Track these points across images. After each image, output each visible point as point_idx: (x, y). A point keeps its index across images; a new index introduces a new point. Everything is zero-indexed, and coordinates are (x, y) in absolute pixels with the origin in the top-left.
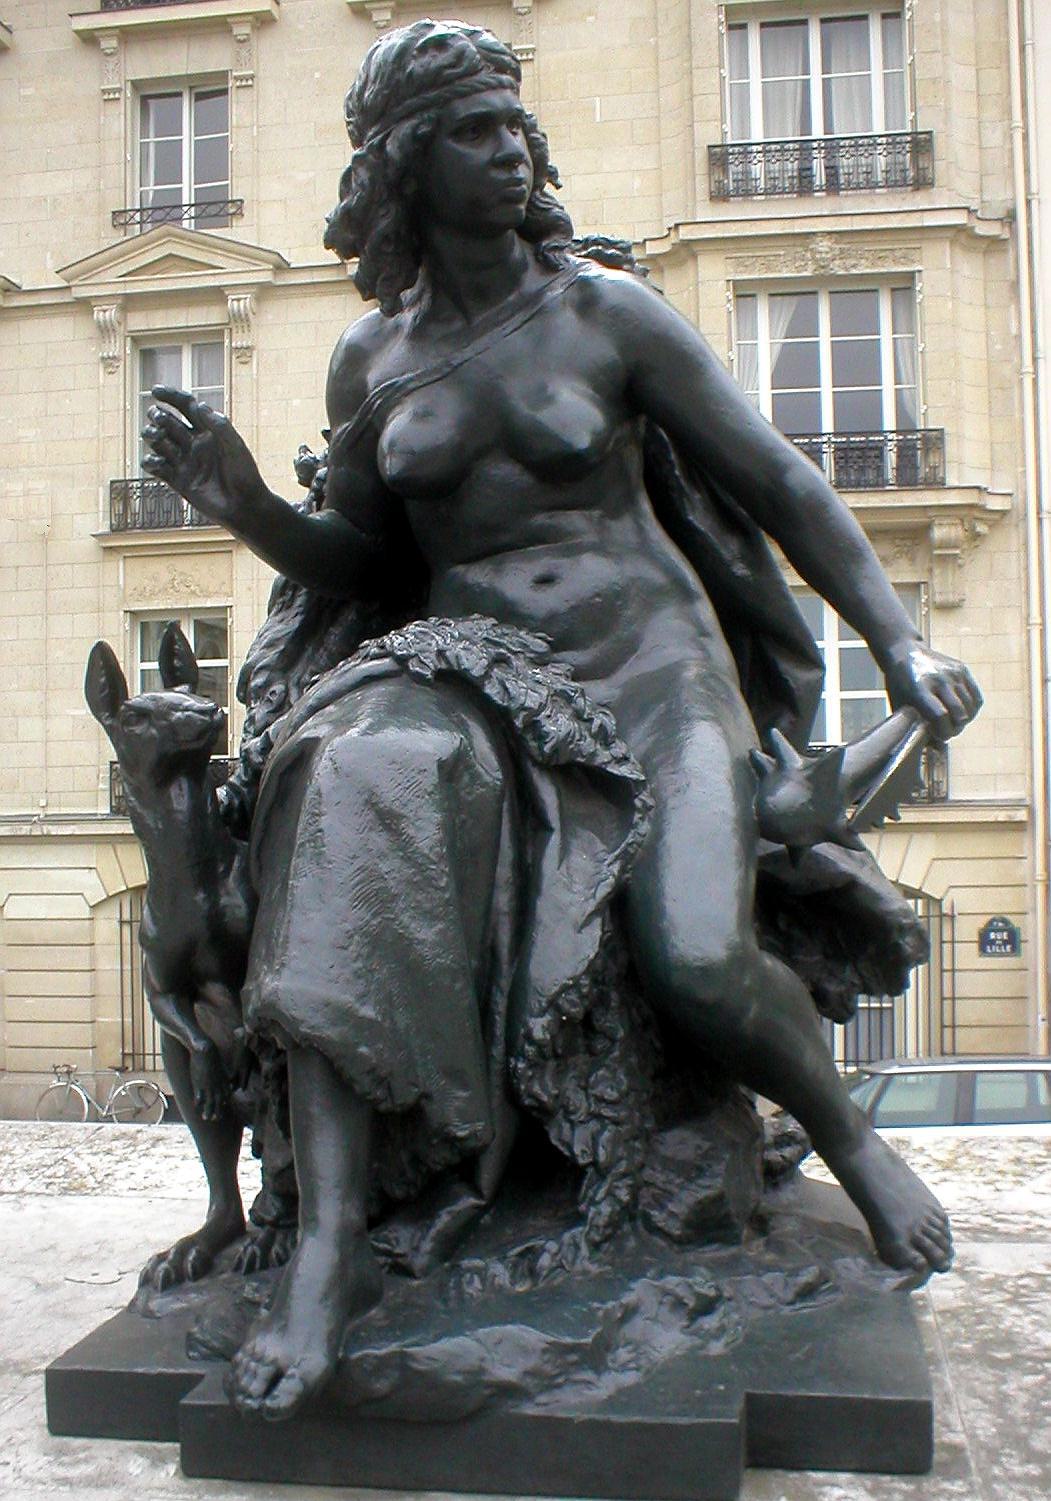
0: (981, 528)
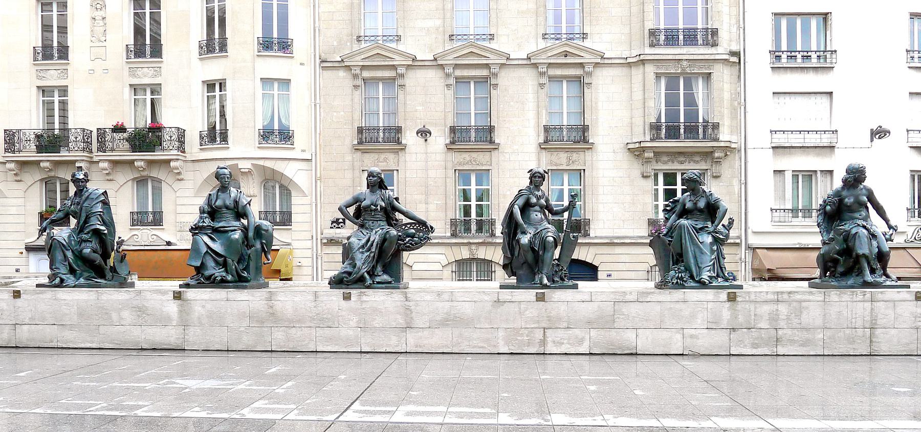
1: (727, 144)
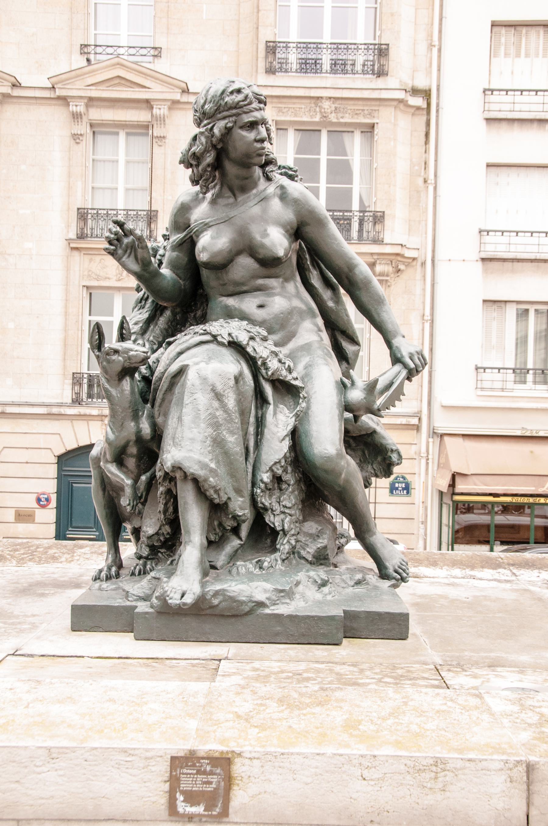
0: (402, 267)
1: (397, 250)
